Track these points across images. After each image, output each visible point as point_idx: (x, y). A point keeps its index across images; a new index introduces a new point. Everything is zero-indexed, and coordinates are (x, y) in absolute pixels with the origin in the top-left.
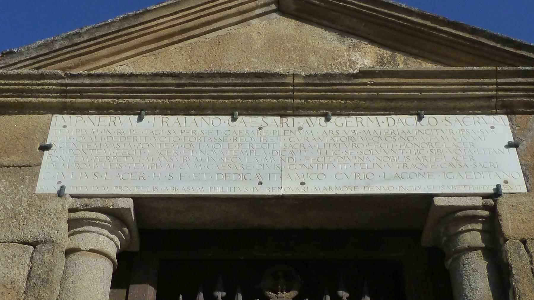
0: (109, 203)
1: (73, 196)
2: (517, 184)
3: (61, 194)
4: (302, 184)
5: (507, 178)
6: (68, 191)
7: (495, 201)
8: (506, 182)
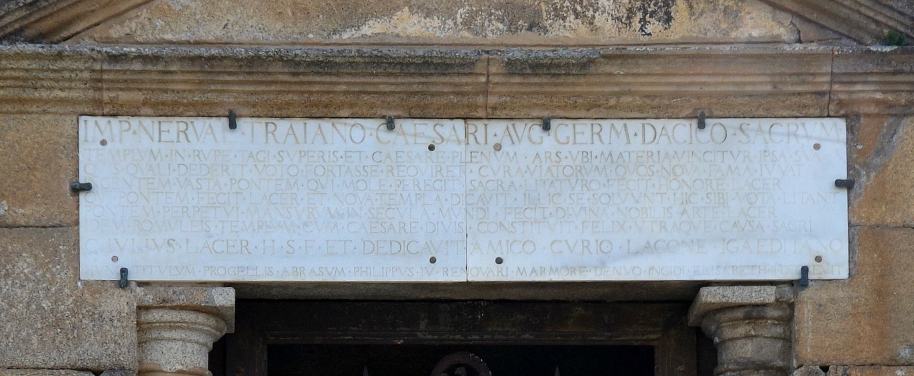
0: (200, 298)
1: (140, 284)
2: (837, 266)
3: (123, 282)
4: (499, 261)
5: (821, 252)
6: (132, 277)
7: (796, 294)
8: (818, 259)
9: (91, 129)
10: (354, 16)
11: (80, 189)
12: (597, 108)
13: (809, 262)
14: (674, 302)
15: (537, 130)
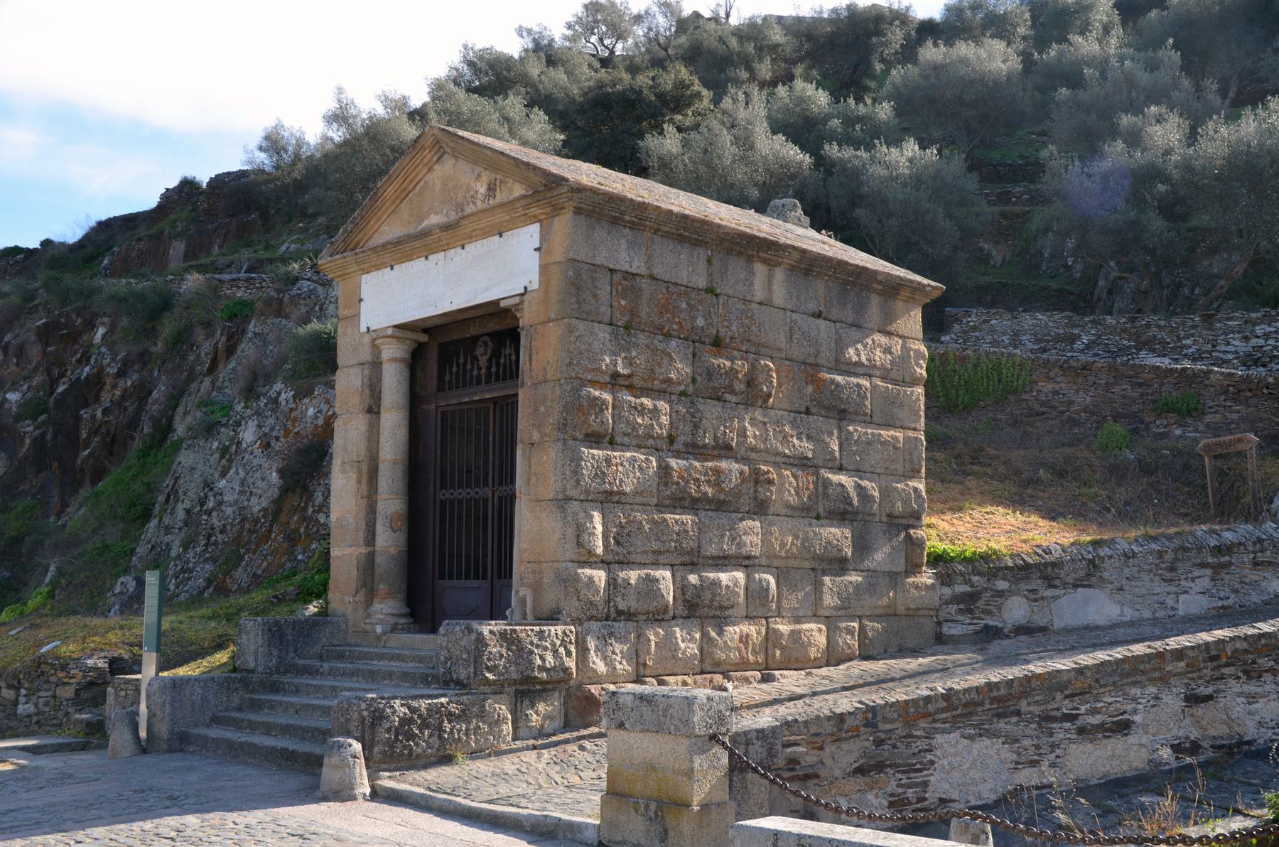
2: (535, 286)
9: (365, 278)
10: (421, 220)
11: (361, 300)
12: (472, 237)
13: (527, 284)
14: (493, 311)
15: (459, 249)
